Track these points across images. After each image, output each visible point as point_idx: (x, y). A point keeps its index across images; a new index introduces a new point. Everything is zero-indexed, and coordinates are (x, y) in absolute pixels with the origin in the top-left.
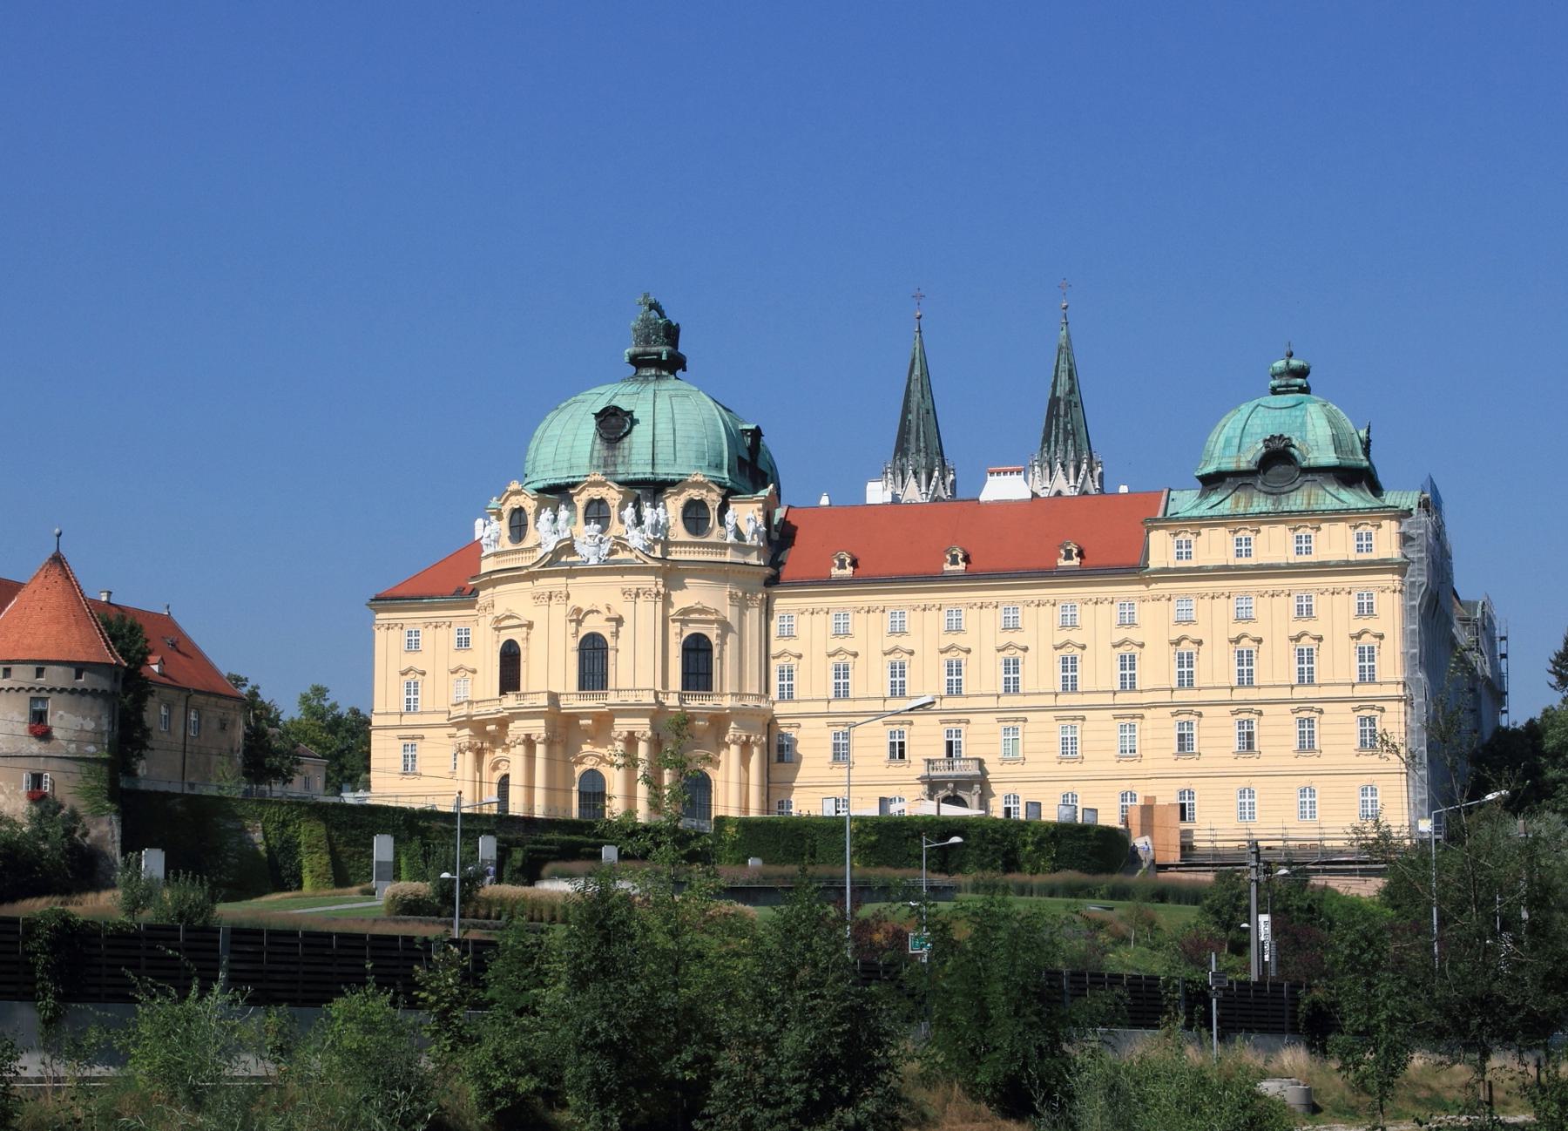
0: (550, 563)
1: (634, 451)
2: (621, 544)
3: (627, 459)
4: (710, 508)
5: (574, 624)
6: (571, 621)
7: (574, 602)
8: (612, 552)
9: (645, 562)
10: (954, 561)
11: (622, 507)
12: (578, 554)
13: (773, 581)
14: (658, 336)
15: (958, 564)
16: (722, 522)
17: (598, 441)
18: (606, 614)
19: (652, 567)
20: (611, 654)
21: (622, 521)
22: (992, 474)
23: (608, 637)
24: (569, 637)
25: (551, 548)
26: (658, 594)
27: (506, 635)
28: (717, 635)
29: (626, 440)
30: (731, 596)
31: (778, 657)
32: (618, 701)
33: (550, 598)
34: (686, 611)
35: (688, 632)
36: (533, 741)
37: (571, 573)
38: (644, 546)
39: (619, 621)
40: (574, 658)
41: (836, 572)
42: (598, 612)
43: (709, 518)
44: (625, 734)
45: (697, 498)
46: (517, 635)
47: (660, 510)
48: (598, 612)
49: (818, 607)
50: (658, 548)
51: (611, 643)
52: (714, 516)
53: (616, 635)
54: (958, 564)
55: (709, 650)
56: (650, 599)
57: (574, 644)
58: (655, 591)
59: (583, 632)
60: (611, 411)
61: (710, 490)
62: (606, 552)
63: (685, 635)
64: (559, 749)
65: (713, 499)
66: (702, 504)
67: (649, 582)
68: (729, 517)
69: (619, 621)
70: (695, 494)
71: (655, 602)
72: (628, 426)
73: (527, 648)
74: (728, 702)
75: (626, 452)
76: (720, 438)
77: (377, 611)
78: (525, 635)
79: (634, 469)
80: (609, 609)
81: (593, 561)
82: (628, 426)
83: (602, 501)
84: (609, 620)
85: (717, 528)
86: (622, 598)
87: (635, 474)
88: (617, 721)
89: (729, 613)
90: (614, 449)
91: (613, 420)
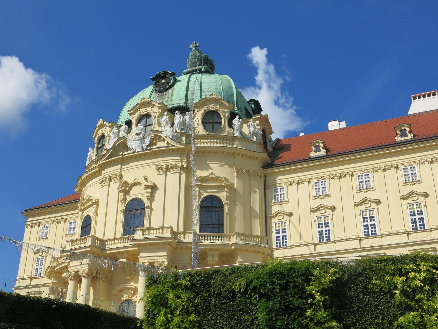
0: (110, 156)
1: (174, 94)
2: (157, 138)
3: (170, 99)
4: (222, 116)
5: (123, 194)
6: (121, 191)
7: (125, 179)
8: (152, 143)
9: (173, 146)
10: (404, 134)
11: (161, 116)
12: (130, 149)
13: (267, 166)
14: (200, 62)
15: (407, 136)
16: (231, 125)
17: (154, 93)
18: (143, 182)
19: (178, 149)
20: (147, 212)
21: (160, 125)
22: (415, 98)
23: (145, 200)
24: (120, 202)
25: (112, 145)
26: (182, 167)
27: (86, 213)
28: (227, 196)
29: (170, 90)
30: (237, 171)
31: (275, 217)
32: (142, 237)
33: (110, 180)
34: (202, 179)
35: (205, 195)
36: (80, 276)
37: (124, 161)
38: (173, 136)
39: (153, 188)
40: (121, 217)
41: (313, 154)
42: (139, 183)
43: (221, 123)
44: (147, 264)
45: (213, 109)
46: (90, 212)
47: (187, 118)
48: (139, 183)
49: (302, 178)
50: (184, 139)
51: (147, 203)
52: (225, 121)
53: (151, 198)
54: (407, 136)
55: (221, 207)
56: (176, 171)
57: (122, 207)
58: (179, 165)
59: (129, 198)
60: (162, 75)
61: (222, 105)
62: (147, 143)
63: (203, 197)
64: (102, 285)
65: (224, 114)
66: (215, 113)
67: (175, 160)
68: (236, 121)
69: (153, 188)
70: (212, 107)
71: (180, 174)
72: (172, 82)
73: (96, 219)
74: (234, 240)
75: (170, 96)
76: (232, 88)
77: (27, 217)
78: (94, 210)
79: (174, 103)
80: (146, 179)
81: (139, 149)
82: (172, 82)
83: (148, 116)
84: (147, 187)
85: (227, 128)
86: (156, 172)
87: (174, 105)
88: (141, 255)
89: (236, 182)
90: (162, 96)
91: (163, 81)
